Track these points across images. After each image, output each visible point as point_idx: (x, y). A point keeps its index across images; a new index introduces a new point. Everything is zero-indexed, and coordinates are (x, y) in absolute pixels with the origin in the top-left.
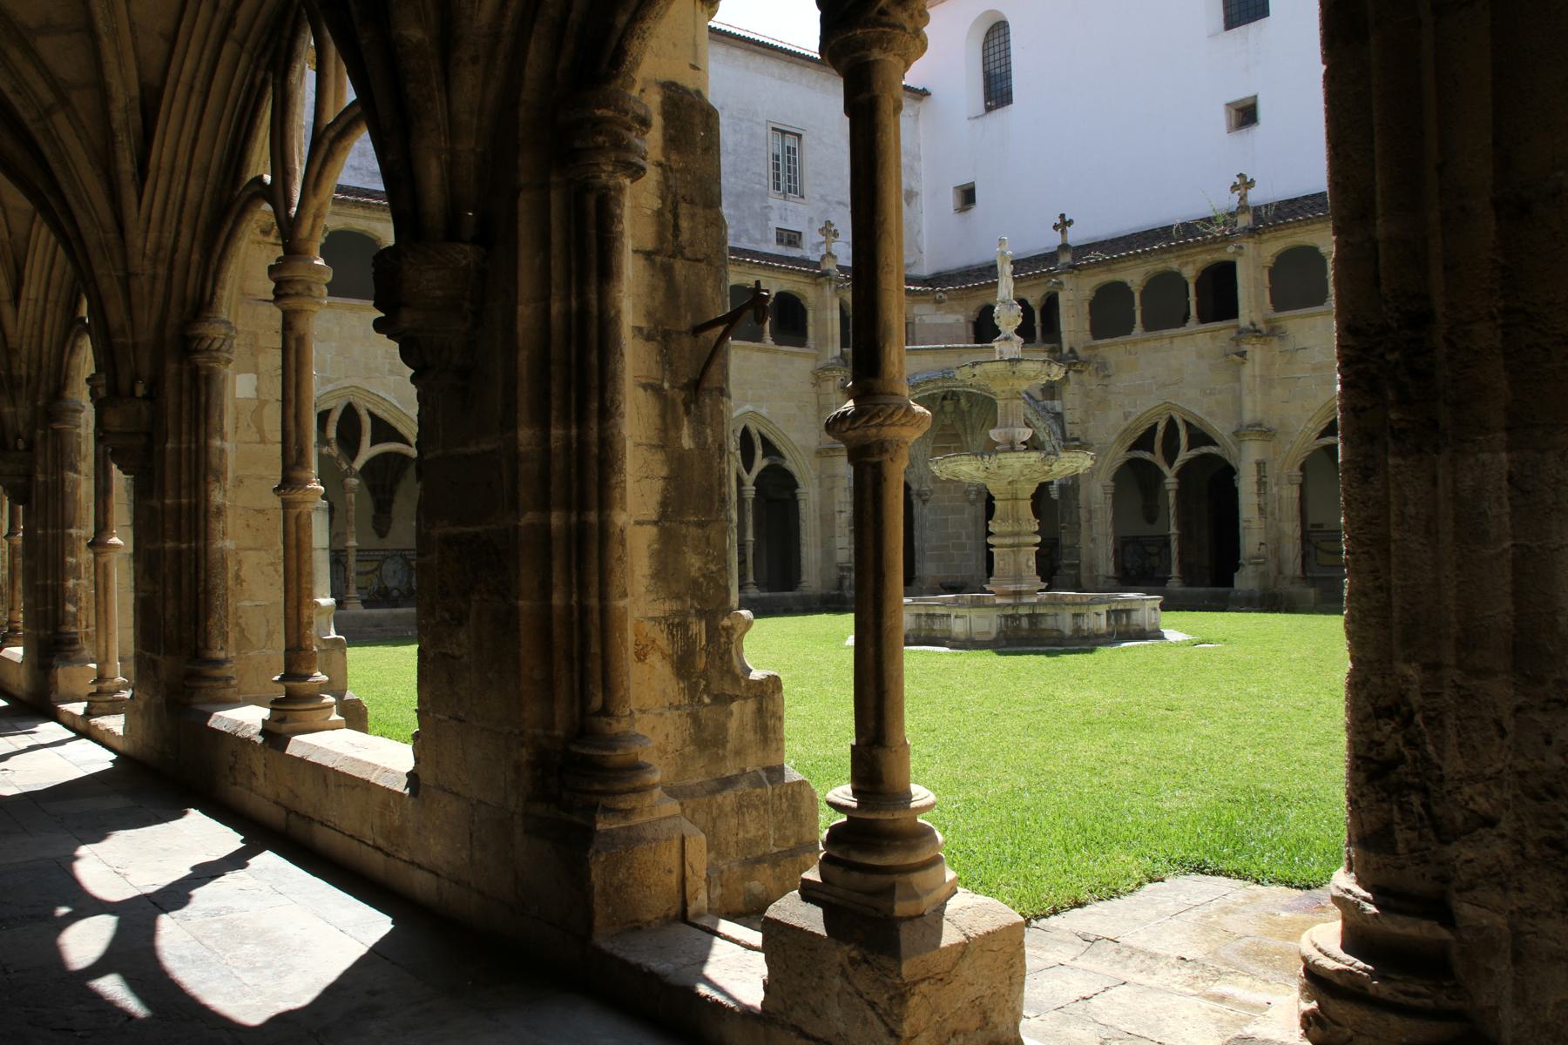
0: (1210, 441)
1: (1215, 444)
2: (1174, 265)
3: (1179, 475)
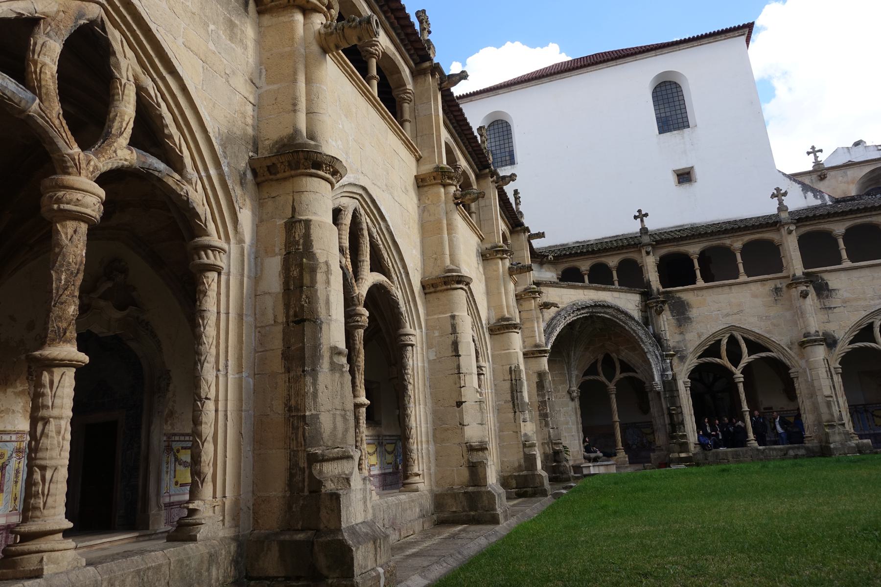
1: (770, 351)
2: (727, 242)
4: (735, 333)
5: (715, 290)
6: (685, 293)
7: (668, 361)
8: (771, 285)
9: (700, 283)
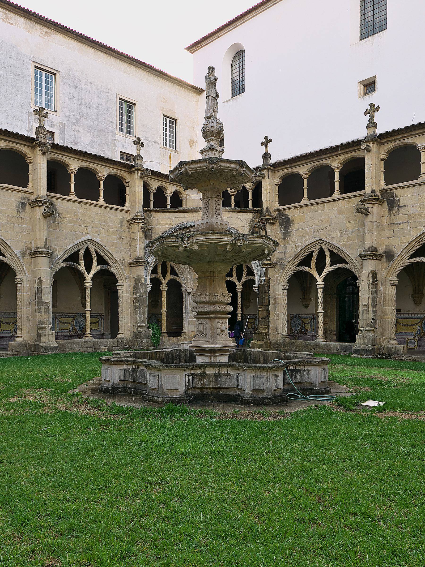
0: (344, 261)
1: (346, 262)
3: (324, 280)
4: (324, 247)
5: (313, 207)
6: (292, 212)
7: (264, 269)
8: (356, 201)
9: (305, 200)
